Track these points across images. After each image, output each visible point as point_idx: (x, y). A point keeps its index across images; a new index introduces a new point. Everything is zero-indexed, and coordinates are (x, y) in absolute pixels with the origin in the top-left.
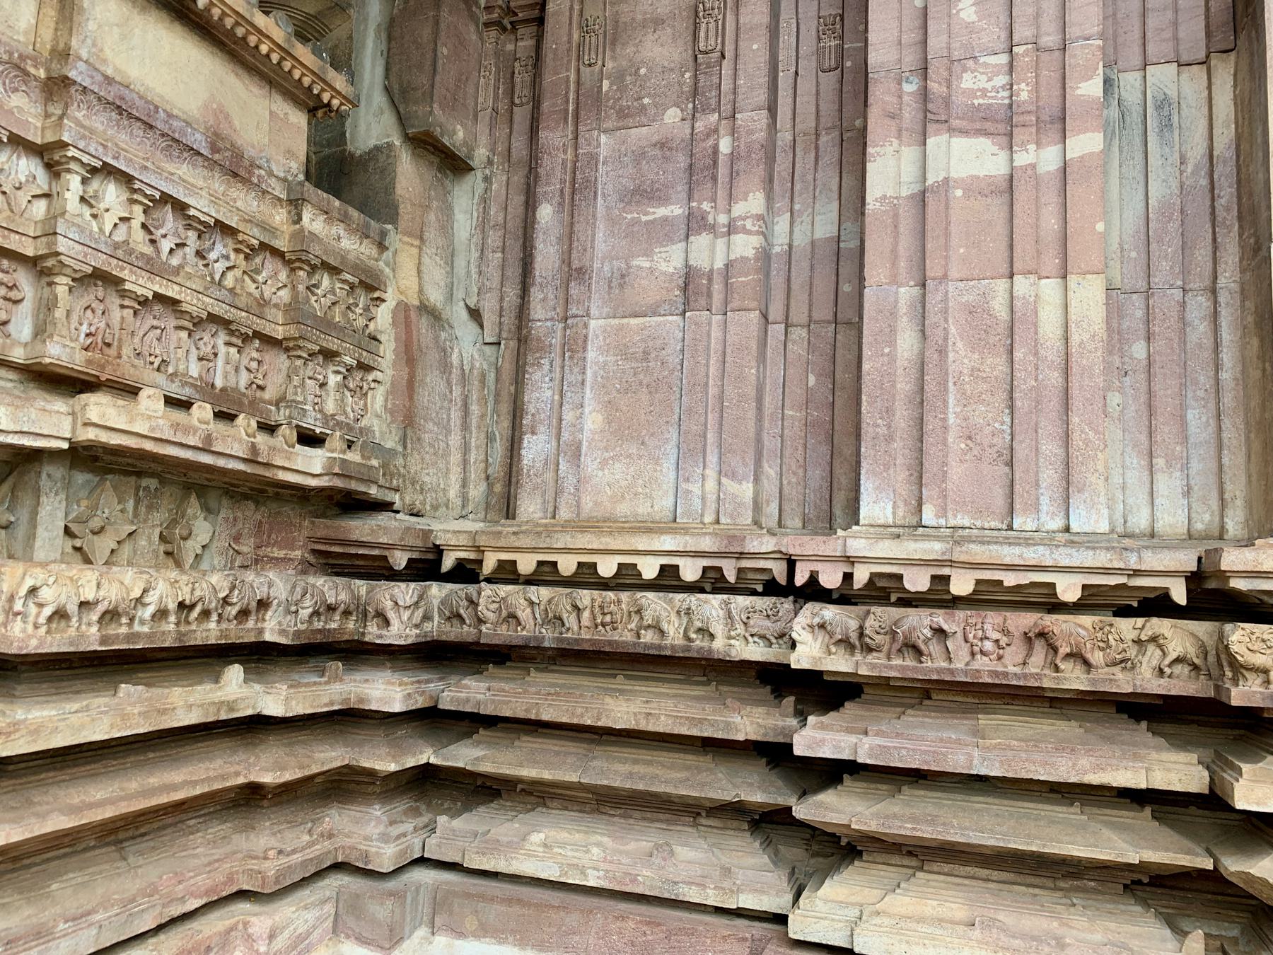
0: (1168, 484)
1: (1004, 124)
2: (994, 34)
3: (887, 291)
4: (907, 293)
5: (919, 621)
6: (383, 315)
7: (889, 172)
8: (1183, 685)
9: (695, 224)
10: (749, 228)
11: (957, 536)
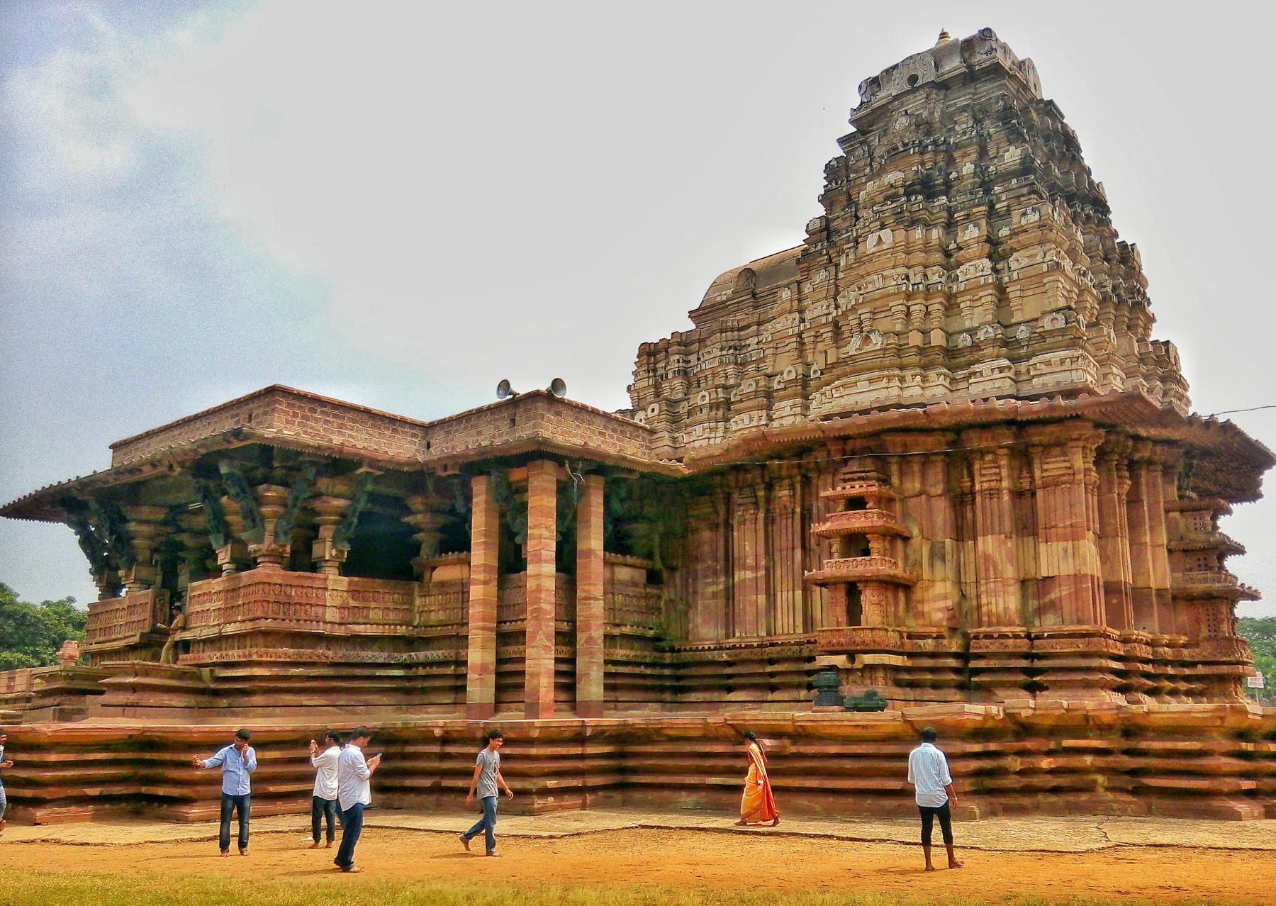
5: (737, 651)
6: (662, 603)
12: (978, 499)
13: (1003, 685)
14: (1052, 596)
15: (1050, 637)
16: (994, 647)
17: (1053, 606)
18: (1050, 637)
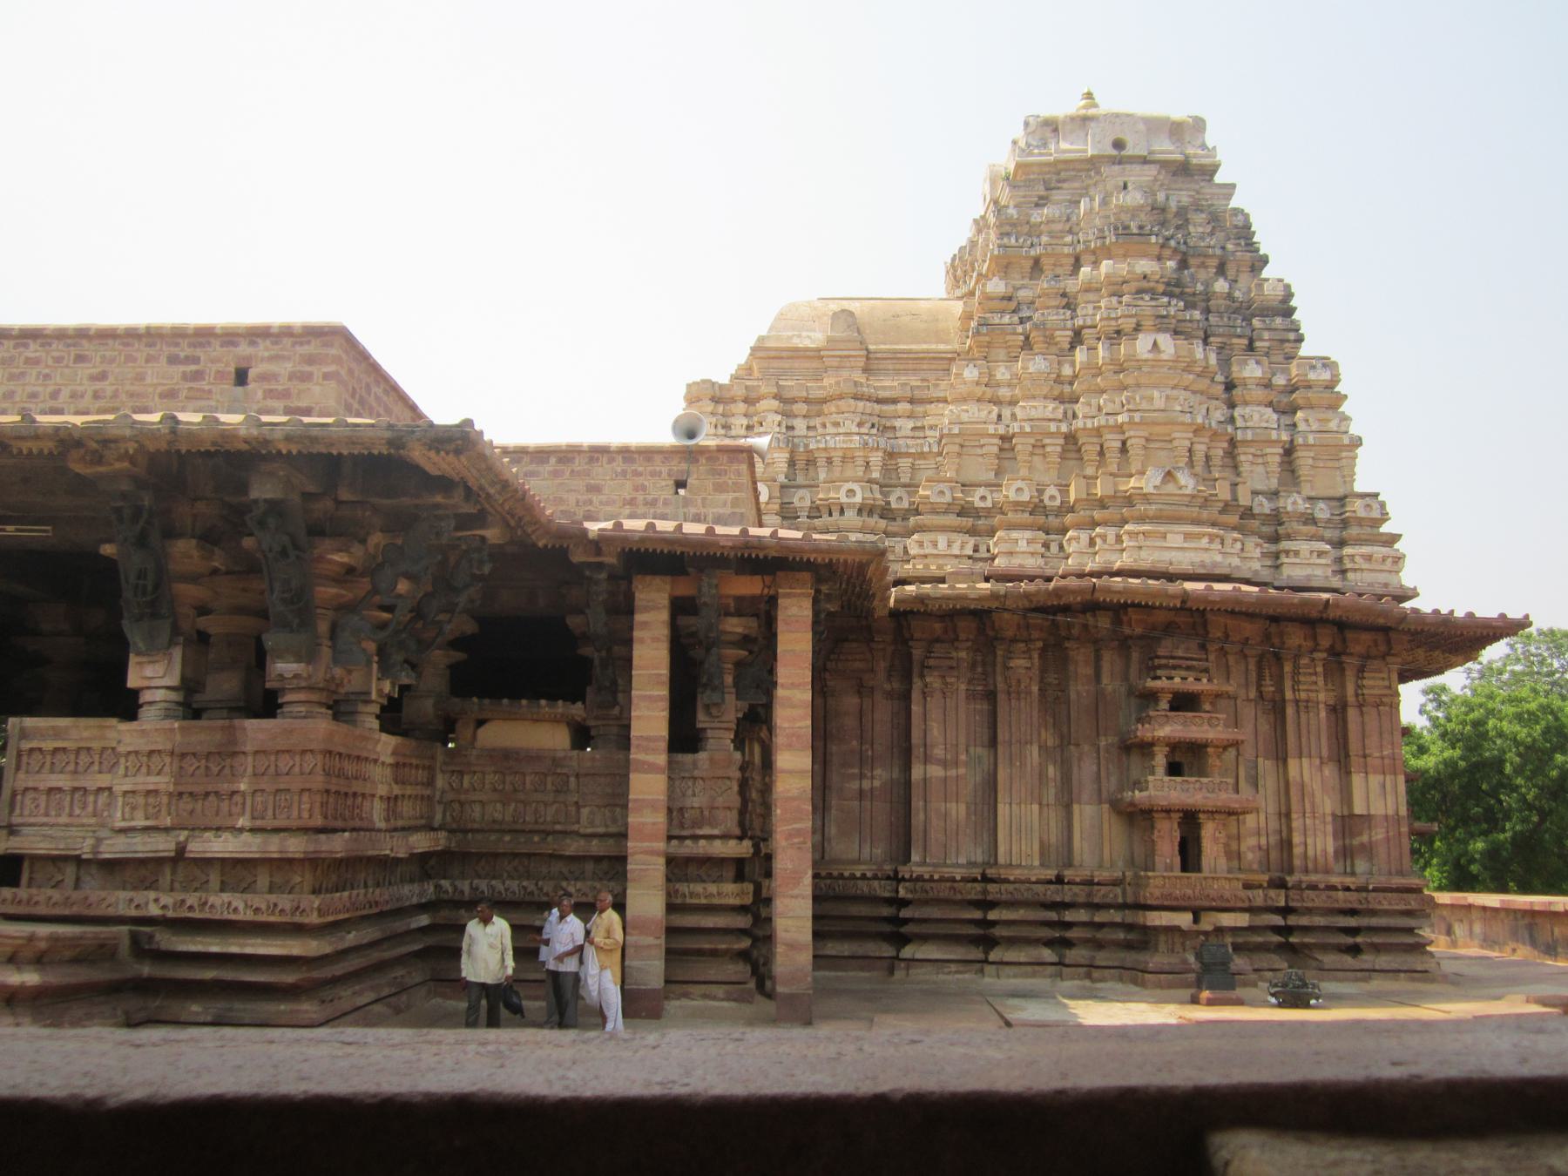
0: (979, 851)
1: (944, 764)
2: (941, 740)
3: (917, 803)
4: (921, 803)
5: (928, 886)
7: (917, 772)
8: (980, 897)
9: (862, 776)
10: (880, 776)
11: (934, 865)
12: (1290, 711)
13: (1325, 948)
14: (1365, 838)
15: (1375, 890)
17: (1368, 850)
18: (1375, 890)
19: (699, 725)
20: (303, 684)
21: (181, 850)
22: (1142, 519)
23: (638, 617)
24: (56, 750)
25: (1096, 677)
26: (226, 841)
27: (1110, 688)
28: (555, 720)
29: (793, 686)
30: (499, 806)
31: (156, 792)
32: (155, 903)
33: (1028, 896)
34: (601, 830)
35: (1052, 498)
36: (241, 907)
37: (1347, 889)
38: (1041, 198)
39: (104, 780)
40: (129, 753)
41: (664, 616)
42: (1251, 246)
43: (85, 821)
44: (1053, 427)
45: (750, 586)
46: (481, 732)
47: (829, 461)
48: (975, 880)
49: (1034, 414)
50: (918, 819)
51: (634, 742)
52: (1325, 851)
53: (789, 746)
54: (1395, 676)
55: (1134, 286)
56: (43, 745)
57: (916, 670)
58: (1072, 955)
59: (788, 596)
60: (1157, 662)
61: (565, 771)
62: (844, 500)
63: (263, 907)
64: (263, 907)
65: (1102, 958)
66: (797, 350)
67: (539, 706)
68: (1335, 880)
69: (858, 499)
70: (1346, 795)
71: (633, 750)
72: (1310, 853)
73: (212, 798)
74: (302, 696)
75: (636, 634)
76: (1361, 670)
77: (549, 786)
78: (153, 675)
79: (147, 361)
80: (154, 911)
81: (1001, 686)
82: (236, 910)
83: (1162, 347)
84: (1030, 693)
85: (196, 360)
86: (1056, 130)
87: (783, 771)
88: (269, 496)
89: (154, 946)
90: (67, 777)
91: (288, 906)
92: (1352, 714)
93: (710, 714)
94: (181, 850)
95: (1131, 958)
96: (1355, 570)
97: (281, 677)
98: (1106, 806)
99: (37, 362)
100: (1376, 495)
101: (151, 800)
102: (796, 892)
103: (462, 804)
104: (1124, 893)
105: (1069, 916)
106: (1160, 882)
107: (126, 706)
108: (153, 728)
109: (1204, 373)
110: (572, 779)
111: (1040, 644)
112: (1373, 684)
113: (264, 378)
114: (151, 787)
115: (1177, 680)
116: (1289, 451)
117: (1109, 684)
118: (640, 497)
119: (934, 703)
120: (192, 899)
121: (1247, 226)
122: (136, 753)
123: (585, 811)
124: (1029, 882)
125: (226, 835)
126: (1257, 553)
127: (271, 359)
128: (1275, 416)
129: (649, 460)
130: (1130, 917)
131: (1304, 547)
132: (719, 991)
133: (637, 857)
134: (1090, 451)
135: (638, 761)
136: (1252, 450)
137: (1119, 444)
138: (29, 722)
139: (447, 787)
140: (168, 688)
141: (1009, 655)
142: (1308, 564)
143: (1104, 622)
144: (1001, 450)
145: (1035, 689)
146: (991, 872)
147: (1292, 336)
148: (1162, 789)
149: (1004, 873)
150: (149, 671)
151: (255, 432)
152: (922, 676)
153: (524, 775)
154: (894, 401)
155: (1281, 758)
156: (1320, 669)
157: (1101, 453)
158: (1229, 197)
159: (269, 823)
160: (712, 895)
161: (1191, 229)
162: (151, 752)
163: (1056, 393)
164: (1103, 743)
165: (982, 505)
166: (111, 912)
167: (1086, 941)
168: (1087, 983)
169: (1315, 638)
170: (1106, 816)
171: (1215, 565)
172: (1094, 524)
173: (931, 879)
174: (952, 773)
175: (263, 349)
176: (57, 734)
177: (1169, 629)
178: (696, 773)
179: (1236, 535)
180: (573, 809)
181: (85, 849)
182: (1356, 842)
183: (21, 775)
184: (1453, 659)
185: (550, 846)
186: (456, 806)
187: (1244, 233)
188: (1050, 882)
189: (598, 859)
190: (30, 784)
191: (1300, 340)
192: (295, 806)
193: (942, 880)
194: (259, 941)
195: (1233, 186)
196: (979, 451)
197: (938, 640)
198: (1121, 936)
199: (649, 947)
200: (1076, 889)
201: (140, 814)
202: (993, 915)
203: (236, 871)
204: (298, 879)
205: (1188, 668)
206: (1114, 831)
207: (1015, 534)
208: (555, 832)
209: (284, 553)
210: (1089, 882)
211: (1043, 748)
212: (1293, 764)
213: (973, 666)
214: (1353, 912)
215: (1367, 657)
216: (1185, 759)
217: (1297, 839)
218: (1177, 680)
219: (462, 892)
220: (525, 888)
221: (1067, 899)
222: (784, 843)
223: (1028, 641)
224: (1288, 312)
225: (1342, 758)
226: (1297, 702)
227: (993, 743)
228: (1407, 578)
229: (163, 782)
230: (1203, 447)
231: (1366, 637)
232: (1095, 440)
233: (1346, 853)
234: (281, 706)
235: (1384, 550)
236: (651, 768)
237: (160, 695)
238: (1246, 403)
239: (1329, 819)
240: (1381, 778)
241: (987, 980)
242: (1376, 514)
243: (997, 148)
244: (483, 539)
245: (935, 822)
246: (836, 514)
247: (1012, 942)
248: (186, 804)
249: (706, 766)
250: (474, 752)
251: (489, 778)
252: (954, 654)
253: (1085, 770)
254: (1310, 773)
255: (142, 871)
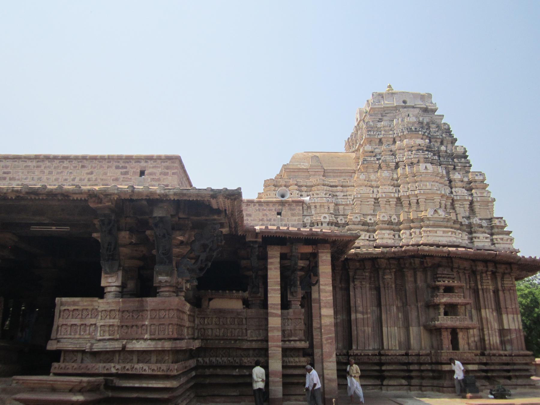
0: (376, 345)
1: (363, 313)
2: (361, 304)
3: (354, 328)
4: (355, 328)
5: (360, 357)
7: (353, 316)
8: (378, 361)
11: (362, 350)
12: (480, 292)
14: (509, 337)
15: (515, 356)
16: (496, 360)
17: (511, 342)
19: (289, 299)
20: (168, 284)
21: (124, 347)
22: (428, 226)
23: (270, 261)
24: (74, 310)
25: (416, 282)
26: (141, 344)
27: (420, 285)
28: (237, 298)
29: (326, 285)
30: (218, 330)
31: (113, 325)
32: (114, 368)
33: (396, 360)
34: (255, 338)
35: (394, 219)
36: (147, 369)
37: (506, 356)
38: (380, 119)
39: (93, 321)
40: (103, 311)
41: (278, 260)
42: (451, 136)
43: (86, 337)
44: (392, 195)
45: (308, 249)
46: (211, 303)
47: (315, 207)
48: (376, 355)
49: (385, 190)
50: (354, 333)
51: (269, 306)
52: (496, 342)
53: (325, 307)
54: (514, 280)
55: (416, 148)
56: (69, 308)
57: (351, 280)
58: (414, 382)
59: (322, 252)
60: (438, 275)
61: (241, 317)
62: (323, 220)
63: (156, 369)
64: (156, 369)
65: (425, 382)
66: (300, 169)
67: (233, 293)
68: (502, 352)
69: (327, 220)
70: (500, 322)
71: (269, 309)
72: (492, 343)
73: (134, 327)
74: (167, 289)
75: (269, 267)
76: (502, 279)
77: (236, 323)
78: (111, 282)
79: (108, 168)
80: (114, 371)
81: (382, 285)
82: (145, 370)
83: (428, 168)
84: (392, 287)
85: (126, 168)
86: (383, 97)
87: (324, 316)
88: (160, 215)
89: (113, 385)
90: (79, 320)
91: (165, 368)
92: (501, 293)
93: (293, 296)
94: (124, 347)
95: (436, 382)
96: (498, 243)
97: (160, 282)
98: (422, 328)
99: (67, 168)
100: (502, 218)
101: (111, 328)
102: (331, 360)
103: (204, 329)
104: (431, 359)
105: (412, 367)
106: (446, 354)
107: (100, 293)
108: (109, 302)
109: (442, 177)
110: (244, 320)
111: (394, 270)
112: (507, 283)
113: (151, 174)
114: (111, 324)
115: (446, 282)
116: (472, 203)
117: (420, 283)
118: (265, 218)
119: (358, 291)
120: (128, 366)
121: (449, 129)
122: (105, 310)
123: (249, 332)
124: (396, 355)
125: (142, 341)
126: (466, 238)
127: (153, 167)
128: (466, 191)
129: (268, 205)
130: (434, 367)
131: (481, 236)
132: (301, 398)
133: (272, 348)
134: (405, 203)
135: (271, 312)
136: (459, 203)
137: (416, 201)
138: (64, 299)
139: (199, 323)
140: (116, 286)
141: (384, 274)
142: (482, 241)
143: (417, 261)
144: (375, 203)
145: (393, 286)
146: (382, 352)
147: (468, 165)
148: (444, 321)
149: (387, 352)
150: (110, 280)
151: (163, 192)
152: (353, 282)
153: (227, 318)
154: (336, 186)
155: (479, 309)
156: (489, 278)
157: (410, 204)
158: (442, 119)
159: (156, 337)
160: (297, 362)
161: (431, 129)
162: (111, 310)
163: (392, 184)
164: (419, 305)
165: (370, 222)
166: (97, 371)
167: (417, 377)
168: (420, 392)
169: (487, 267)
170: (422, 331)
171: (454, 242)
172: (411, 228)
173: (361, 355)
174: (365, 316)
175: (150, 164)
176: (75, 304)
177: (439, 265)
178: (289, 317)
179: (459, 231)
180: (244, 331)
181: (87, 347)
182: (506, 339)
183: (61, 319)
184: (529, 273)
185: (238, 345)
186: (203, 330)
187: (448, 131)
188: (403, 355)
189: (254, 349)
190: (64, 323)
191: (470, 166)
192: (167, 331)
193: (365, 355)
194: (154, 382)
195: (443, 116)
196: (367, 203)
197: (358, 269)
198: (431, 374)
199: (277, 381)
200: (413, 357)
201: (107, 334)
202: (384, 368)
203: (143, 355)
204: (167, 358)
205: (448, 278)
206: (425, 336)
207: (383, 232)
208: (239, 340)
209: (164, 236)
210: (418, 355)
211: (397, 307)
212: (483, 311)
213: (370, 278)
214: (507, 364)
215: (504, 274)
216: (451, 309)
217: (486, 338)
218: (446, 282)
219: (206, 363)
220: (229, 360)
221: (410, 361)
222: (325, 342)
223: (390, 269)
224: (466, 157)
225: (499, 310)
226: (483, 289)
227: (379, 305)
228: (515, 246)
229: (116, 322)
230: (444, 202)
231: (503, 266)
232: (407, 199)
233: (503, 343)
234: (158, 293)
235: (507, 237)
236: (276, 315)
237: (113, 289)
238: (456, 187)
239: (497, 331)
240: (512, 316)
241: (383, 392)
242: (503, 224)
243: (361, 101)
244: (222, 232)
245: (361, 334)
246: (320, 225)
247: (391, 377)
248: (125, 330)
249: (292, 314)
250: (209, 310)
251: (214, 320)
252: (364, 274)
253: (413, 315)
254: (488, 314)
255: (107, 356)
